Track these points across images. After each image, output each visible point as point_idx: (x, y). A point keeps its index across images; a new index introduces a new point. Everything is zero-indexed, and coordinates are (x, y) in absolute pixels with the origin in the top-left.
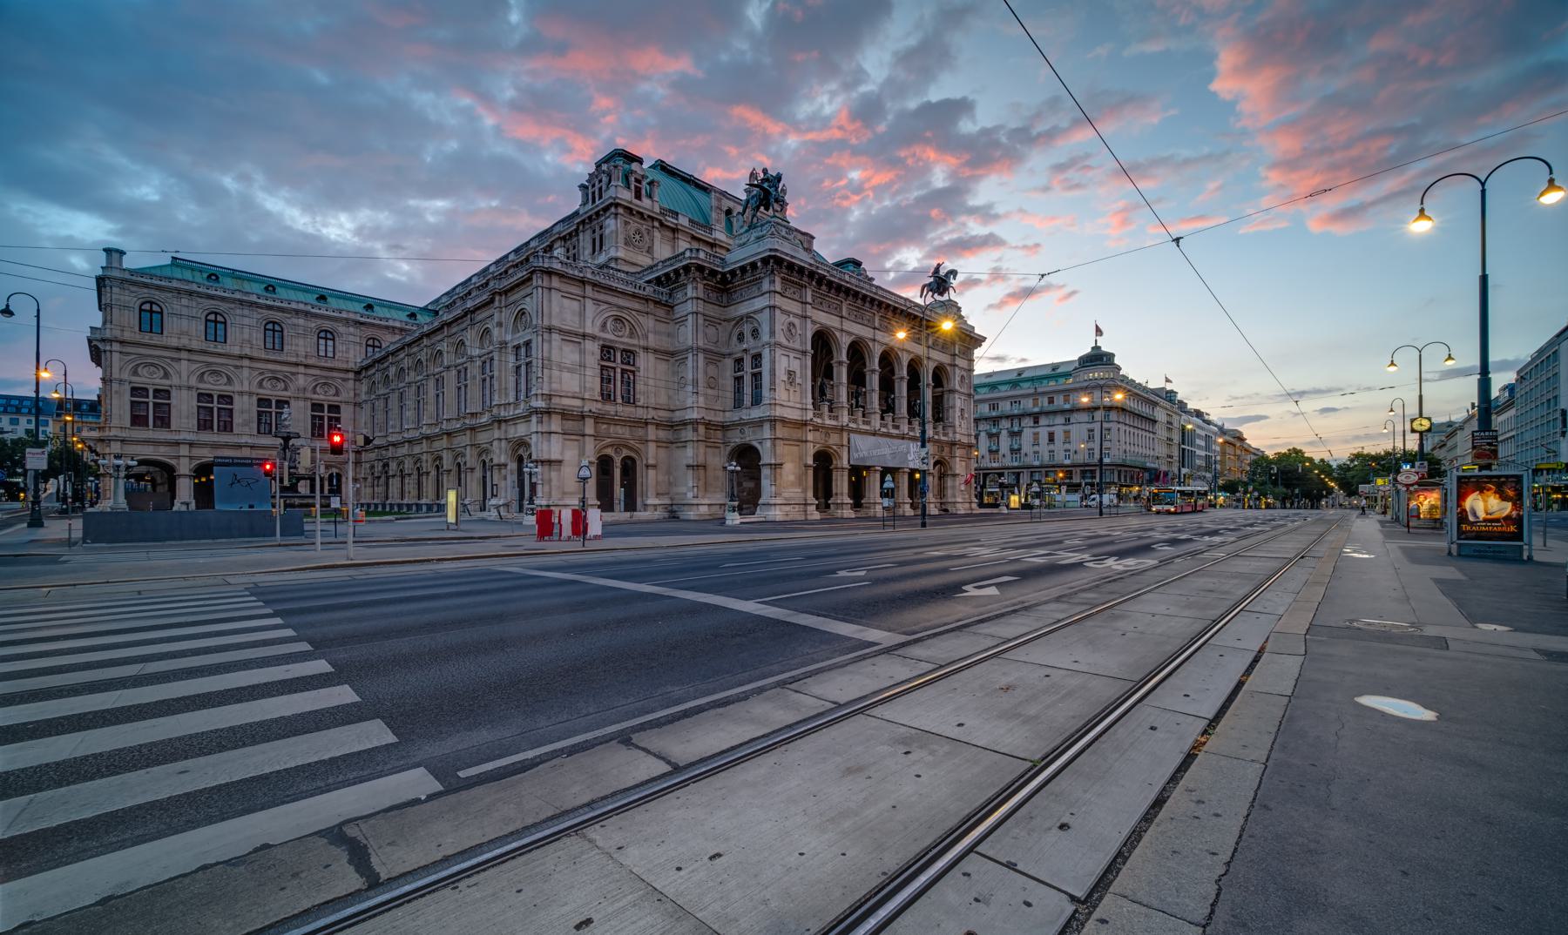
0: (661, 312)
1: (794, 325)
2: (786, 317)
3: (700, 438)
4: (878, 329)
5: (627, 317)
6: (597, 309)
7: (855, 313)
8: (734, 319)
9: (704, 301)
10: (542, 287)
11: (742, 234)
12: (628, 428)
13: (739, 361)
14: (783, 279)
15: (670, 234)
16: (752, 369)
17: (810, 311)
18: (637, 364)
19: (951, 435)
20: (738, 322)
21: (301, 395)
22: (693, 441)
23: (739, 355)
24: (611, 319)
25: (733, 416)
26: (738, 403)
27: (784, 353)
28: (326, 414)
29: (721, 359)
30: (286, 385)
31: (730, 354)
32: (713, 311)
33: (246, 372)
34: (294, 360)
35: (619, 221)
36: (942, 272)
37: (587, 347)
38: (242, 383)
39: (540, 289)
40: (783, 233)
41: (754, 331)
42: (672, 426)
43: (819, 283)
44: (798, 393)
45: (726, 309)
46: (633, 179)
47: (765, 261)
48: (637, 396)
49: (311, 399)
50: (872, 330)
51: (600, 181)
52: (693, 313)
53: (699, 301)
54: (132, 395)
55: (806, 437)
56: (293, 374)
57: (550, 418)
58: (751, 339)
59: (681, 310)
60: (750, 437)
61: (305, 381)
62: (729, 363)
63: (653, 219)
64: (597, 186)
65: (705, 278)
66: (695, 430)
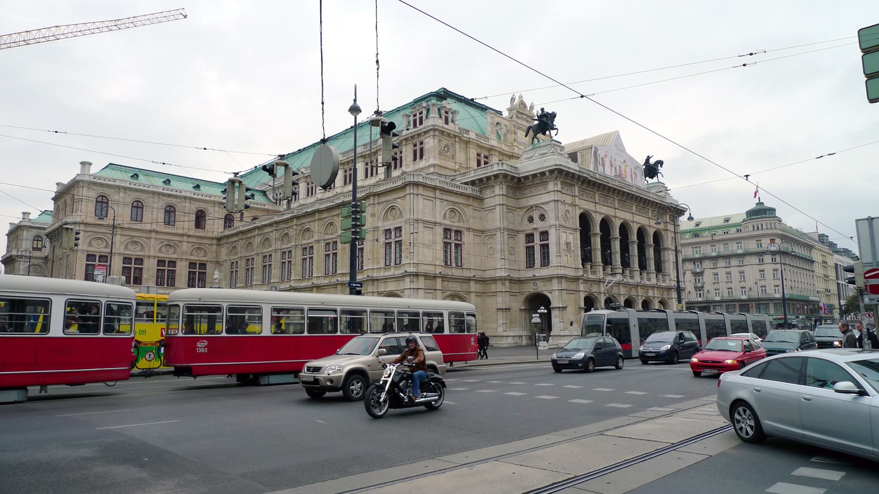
0: (476, 204)
1: (568, 212)
2: (564, 206)
4: (617, 209)
5: (457, 209)
6: (442, 204)
7: (603, 199)
8: (525, 207)
9: (507, 196)
10: (413, 194)
11: (528, 151)
12: (459, 283)
14: (562, 182)
15: (463, 145)
16: (540, 241)
17: (578, 201)
18: (463, 239)
19: (668, 281)
20: (528, 209)
21: (184, 257)
22: (502, 292)
24: (449, 211)
25: (529, 274)
26: (530, 264)
28: (197, 270)
29: (517, 234)
30: (175, 250)
31: (524, 231)
32: (512, 202)
33: (153, 241)
34: (181, 232)
35: (436, 140)
37: (437, 230)
38: (150, 249)
39: (412, 195)
40: (559, 151)
41: (541, 216)
42: (483, 281)
43: (583, 182)
44: (573, 257)
45: (518, 201)
47: (552, 172)
49: (190, 260)
50: (614, 210)
51: (421, 113)
52: (500, 205)
53: (504, 197)
54: (87, 260)
55: (579, 288)
56: (180, 242)
57: (418, 279)
58: (539, 221)
59: (488, 203)
60: (542, 288)
61: (187, 247)
62: (522, 238)
63: (455, 136)
64: (418, 116)
65: (508, 182)
66: (503, 284)
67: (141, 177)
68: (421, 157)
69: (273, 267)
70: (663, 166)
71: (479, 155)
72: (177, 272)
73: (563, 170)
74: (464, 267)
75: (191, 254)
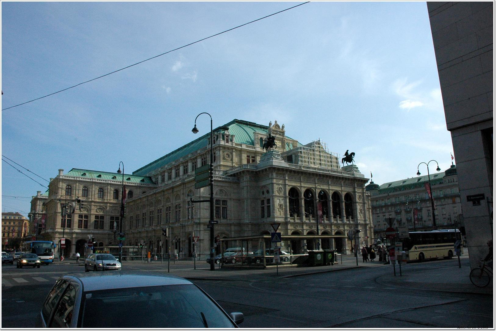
1: (282, 189)
3: (249, 230)
5: (224, 189)
7: (307, 179)
13: (263, 201)
14: (276, 173)
15: (238, 152)
18: (228, 204)
21: (108, 214)
23: (263, 199)
26: (263, 216)
27: (278, 198)
36: (349, 153)
40: (276, 157)
46: (225, 136)
48: (228, 216)
62: (259, 202)
63: (232, 149)
67: (87, 174)
68: (215, 161)
69: (146, 219)
70: (355, 156)
71: (248, 156)
72: (105, 222)
73: (275, 168)
74: (228, 218)
75: (112, 213)
